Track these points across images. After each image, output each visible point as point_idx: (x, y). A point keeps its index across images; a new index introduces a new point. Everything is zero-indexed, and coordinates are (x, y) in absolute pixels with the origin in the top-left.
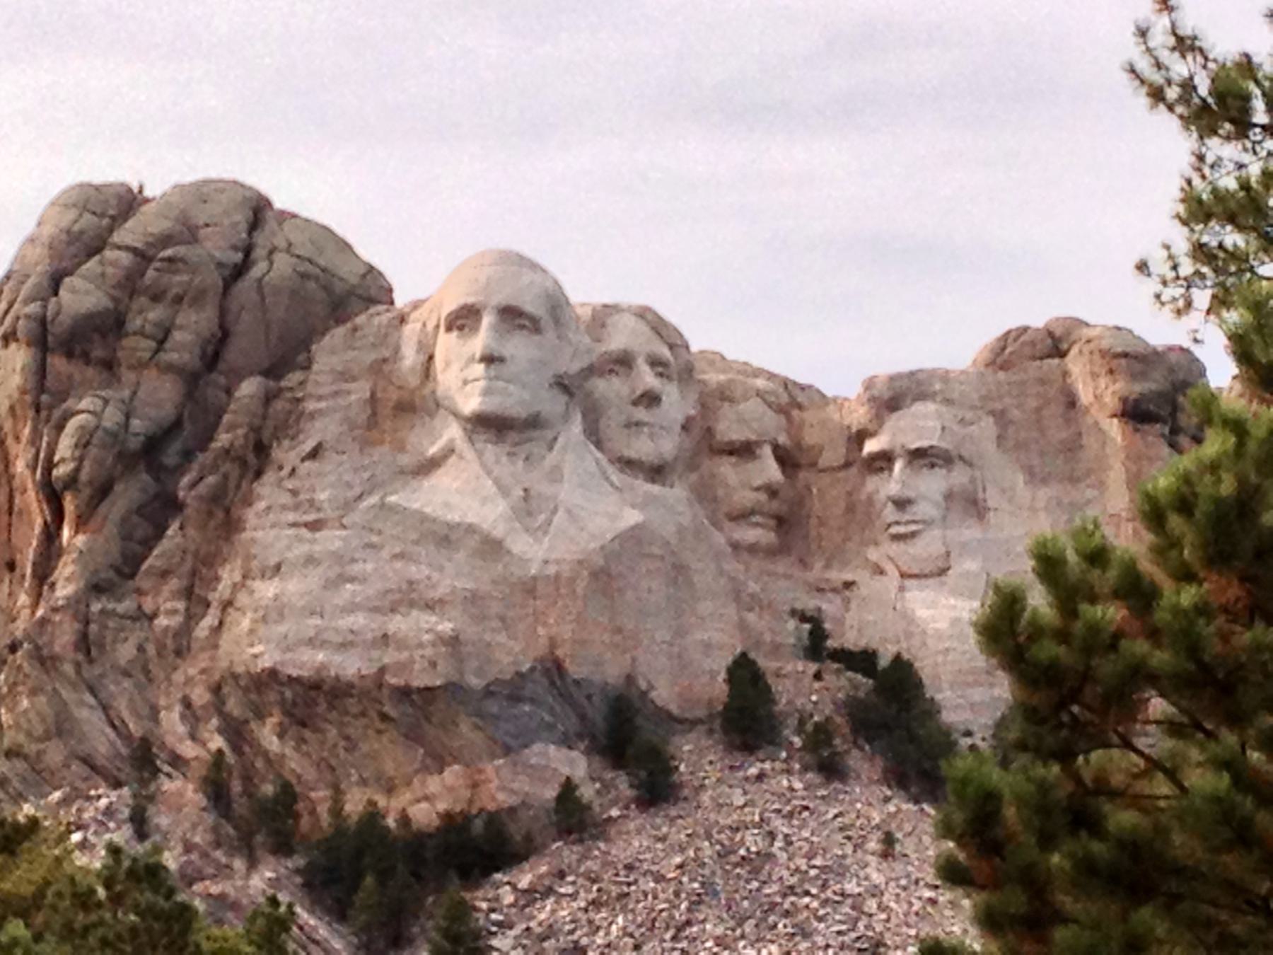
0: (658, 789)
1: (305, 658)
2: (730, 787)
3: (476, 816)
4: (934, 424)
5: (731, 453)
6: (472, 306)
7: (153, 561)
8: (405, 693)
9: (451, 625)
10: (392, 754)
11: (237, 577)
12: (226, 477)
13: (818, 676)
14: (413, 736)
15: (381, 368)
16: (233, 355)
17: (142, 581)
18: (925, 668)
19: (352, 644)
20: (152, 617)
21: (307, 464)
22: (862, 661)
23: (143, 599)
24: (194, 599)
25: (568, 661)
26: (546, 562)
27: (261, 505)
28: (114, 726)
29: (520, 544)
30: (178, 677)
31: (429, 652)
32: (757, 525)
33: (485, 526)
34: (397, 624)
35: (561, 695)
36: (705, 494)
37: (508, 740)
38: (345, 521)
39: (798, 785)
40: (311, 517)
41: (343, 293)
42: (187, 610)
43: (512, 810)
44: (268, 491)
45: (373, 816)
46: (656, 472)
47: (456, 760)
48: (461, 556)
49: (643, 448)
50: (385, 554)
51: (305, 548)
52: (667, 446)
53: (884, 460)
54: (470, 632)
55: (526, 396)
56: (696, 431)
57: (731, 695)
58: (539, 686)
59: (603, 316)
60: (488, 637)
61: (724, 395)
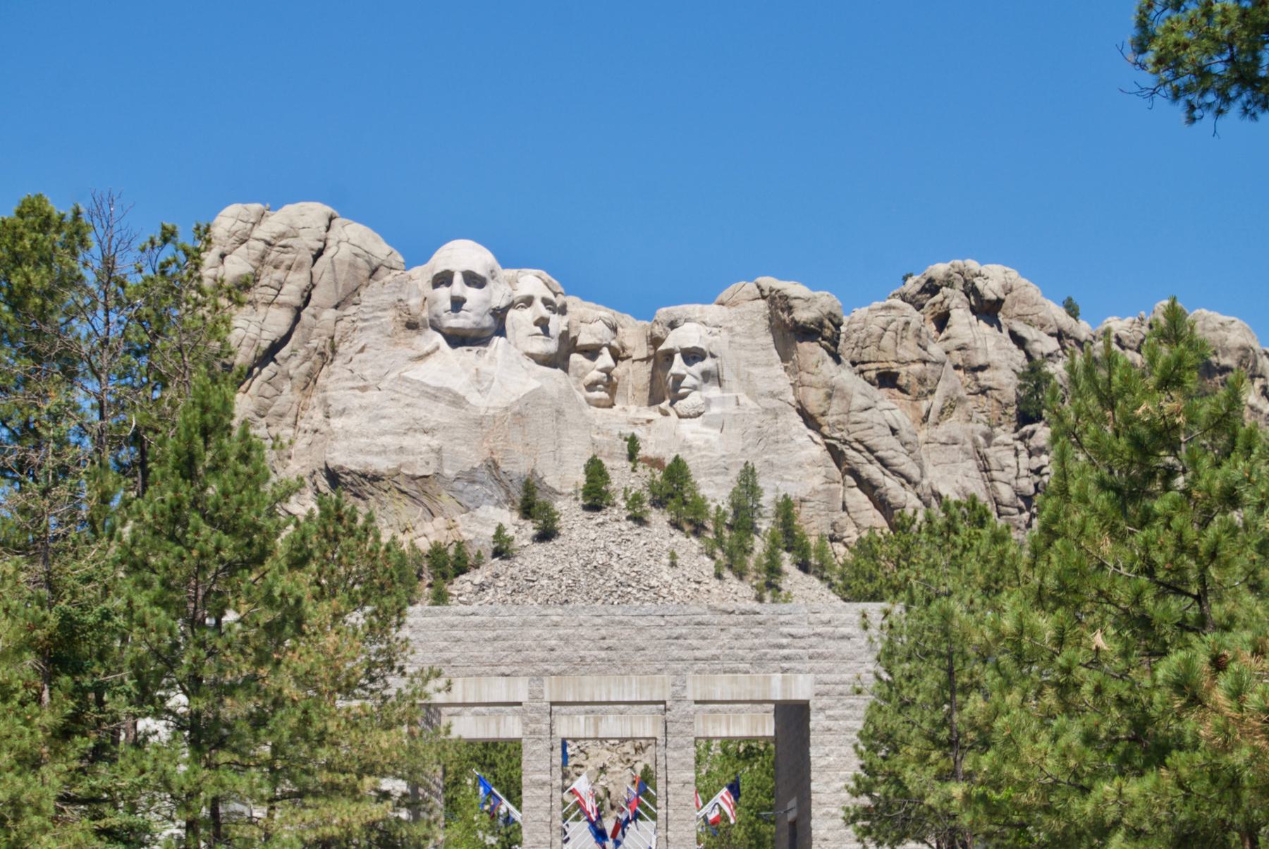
4: (697, 335)
8: (414, 478)
12: (315, 363)
13: (633, 470)
19: (385, 452)
27: (333, 378)
29: (474, 398)
32: (600, 390)
34: (408, 441)
39: (624, 528)
40: (362, 384)
43: (471, 541)
48: (442, 405)
52: (551, 346)
54: (447, 446)
55: (477, 319)
57: (588, 481)
58: (484, 476)
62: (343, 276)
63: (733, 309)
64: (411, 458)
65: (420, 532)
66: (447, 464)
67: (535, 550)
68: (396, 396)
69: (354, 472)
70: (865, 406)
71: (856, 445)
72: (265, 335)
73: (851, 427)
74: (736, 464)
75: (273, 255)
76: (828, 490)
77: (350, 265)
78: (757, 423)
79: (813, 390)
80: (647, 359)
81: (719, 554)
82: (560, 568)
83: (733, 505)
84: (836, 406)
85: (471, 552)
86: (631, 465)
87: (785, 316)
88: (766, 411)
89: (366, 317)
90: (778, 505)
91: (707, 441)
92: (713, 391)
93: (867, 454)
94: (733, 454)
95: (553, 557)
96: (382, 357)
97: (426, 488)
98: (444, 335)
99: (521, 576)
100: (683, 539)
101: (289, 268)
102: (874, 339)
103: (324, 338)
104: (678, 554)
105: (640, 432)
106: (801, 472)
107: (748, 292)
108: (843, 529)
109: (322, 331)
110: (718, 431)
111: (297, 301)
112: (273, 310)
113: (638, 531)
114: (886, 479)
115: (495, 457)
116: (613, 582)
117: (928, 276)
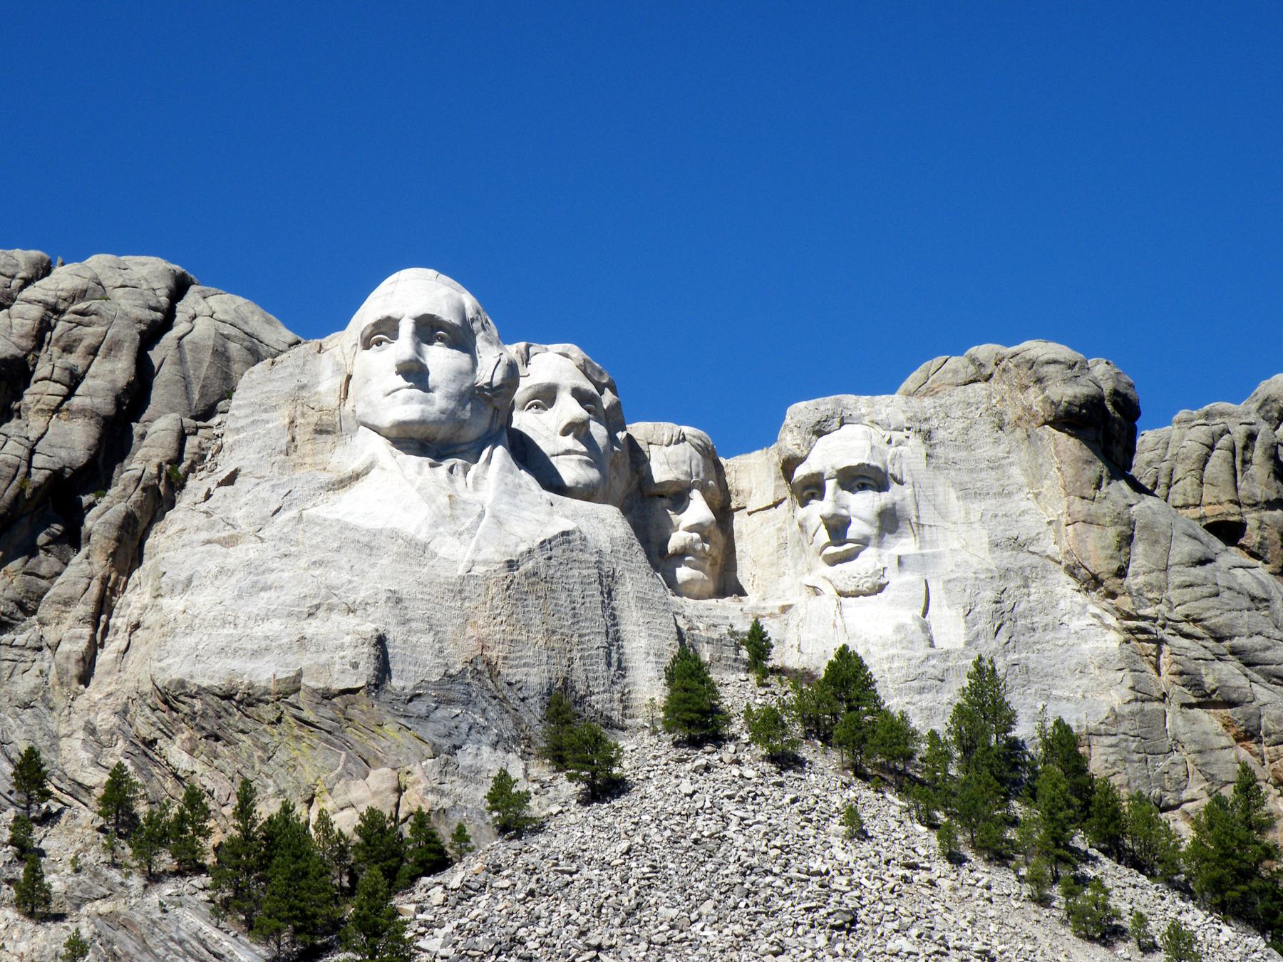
1: (217, 667)
2: (677, 777)
3: (405, 820)
5: (661, 496)
6: (389, 318)
7: (58, 589)
9: (374, 626)
11: (147, 599)
15: (300, 393)
17: (45, 611)
20: (54, 647)
21: (222, 488)
23: (47, 628)
25: (500, 662)
26: (474, 562)
27: (172, 530)
28: (11, 761)
30: (81, 703)
31: (349, 653)
33: (411, 531)
35: (495, 698)
37: (437, 741)
38: (260, 534)
39: (749, 773)
42: (93, 637)
47: (383, 764)
48: (385, 561)
50: (303, 562)
51: (219, 560)
54: (395, 636)
56: (626, 470)
60: (414, 639)
62: (203, 369)
63: (927, 402)
64: (324, 658)
65: (341, 801)
66: (395, 667)
67: (572, 819)
68: (293, 549)
69: (208, 691)
70: (1198, 555)
71: (1187, 628)
72: (38, 460)
73: (1174, 595)
74: (958, 671)
75: (61, 327)
76: (1142, 710)
77: (216, 352)
78: (989, 594)
79: (1095, 528)
80: (776, 505)
81: (941, 816)
82: (624, 845)
83: (960, 737)
84: (1140, 556)
85: (445, 833)
86: (753, 678)
87: (1034, 397)
88: (1005, 574)
89: (239, 425)
90: (1047, 744)
91: (900, 628)
92: (904, 545)
93: (1211, 644)
94: (948, 652)
95: (610, 827)
96: (267, 485)
97: (351, 712)
98: (387, 438)
99: (546, 866)
100: (871, 793)
101: (94, 351)
102: (1189, 465)
103: (156, 461)
104: (865, 816)
106: (1085, 681)
107: (956, 372)
108: (1180, 786)
109: (152, 452)
110: (919, 612)
111: (105, 405)
112: (58, 425)
113: (778, 779)
114: (1256, 687)
115: (493, 654)
116: (733, 868)
117: (1261, 397)
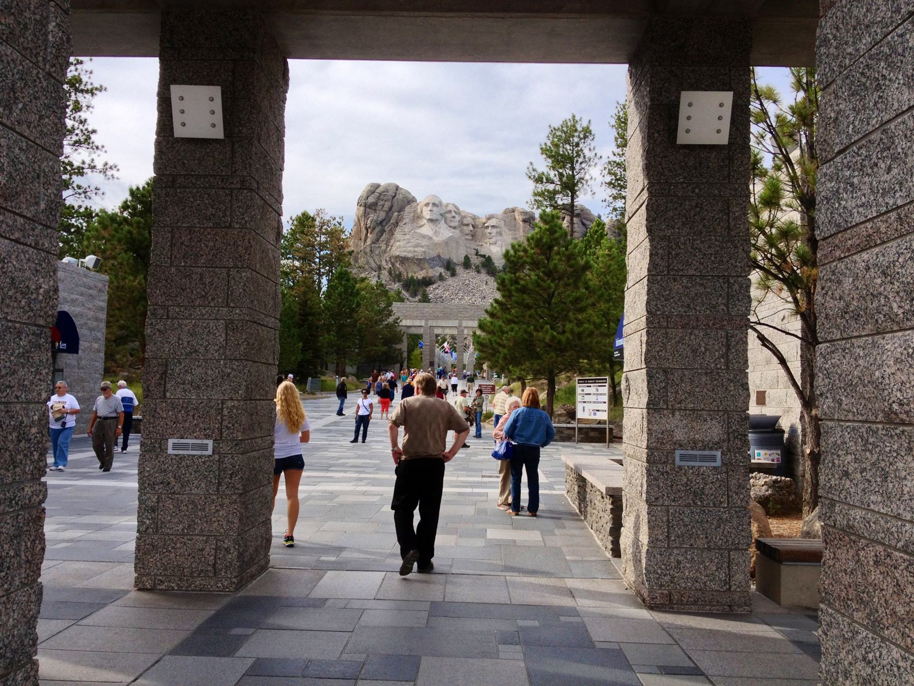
0: (453, 274)
10: (416, 268)
14: (419, 265)
16: (393, 209)
18: (493, 257)
22: (484, 256)
24: (387, 245)
29: (435, 238)
36: (462, 231)
41: (410, 200)
44: (398, 229)
45: (412, 277)
46: (454, 228)
49: (453, 224)
53: (488, 227)
59: (447, 205)
61: (465, 217)
105: (479, 248)
